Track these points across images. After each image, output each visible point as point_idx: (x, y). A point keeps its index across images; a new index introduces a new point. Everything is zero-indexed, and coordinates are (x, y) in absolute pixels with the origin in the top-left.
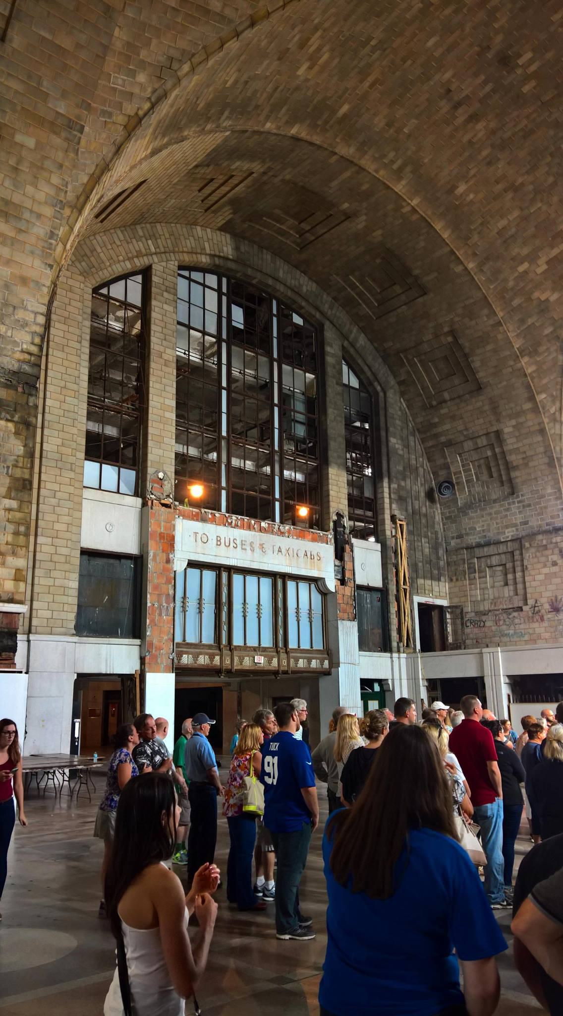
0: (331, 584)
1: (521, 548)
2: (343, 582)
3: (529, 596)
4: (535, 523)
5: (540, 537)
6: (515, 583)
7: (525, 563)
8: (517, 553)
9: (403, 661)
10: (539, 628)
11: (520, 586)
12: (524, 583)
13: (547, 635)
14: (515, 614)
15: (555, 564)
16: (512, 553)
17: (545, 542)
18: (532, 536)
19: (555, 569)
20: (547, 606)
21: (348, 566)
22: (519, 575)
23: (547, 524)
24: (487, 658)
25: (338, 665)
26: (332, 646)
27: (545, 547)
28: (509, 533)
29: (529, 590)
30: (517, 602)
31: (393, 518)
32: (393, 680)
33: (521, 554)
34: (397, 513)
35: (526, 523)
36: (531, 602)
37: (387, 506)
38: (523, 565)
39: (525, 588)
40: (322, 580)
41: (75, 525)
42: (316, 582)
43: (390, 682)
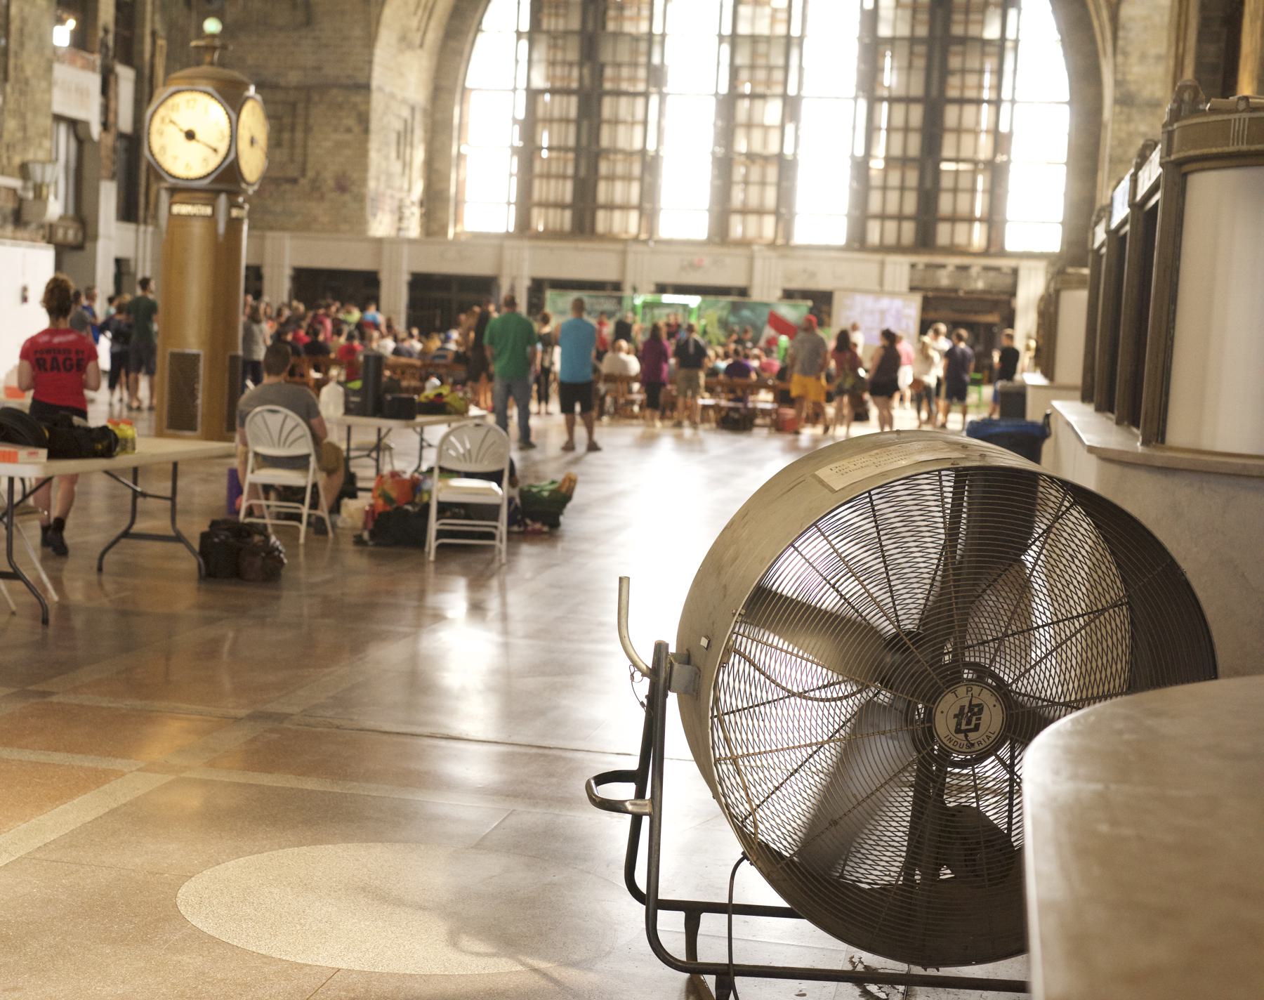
0: (96, 130)
1: (308, 100)
2: (105, 126)
3: (309, 165)
4: (331, 71)
5: (335, 91)
6: (292, 145)
7: (311, 121)
8: (300, 106)
9: (149, 237)
10: (317, 209)
11: (299, 151)
12: (305, 146)
13: (325, 219)
14: (287, 187)
15: (349, 130)
16: (294, 106)
17: (340, 99)
18: (324, 88)
19: (348, 137)
20: (331, 183)
21: (112, 105)
22: (299, 135)
23: (348, 77)
24: (269, 244)
25: (95, 238)
26: (86, 211)
27: (340, 106)
28: (294, 77)
29: (311, 159)
30: (292, 171)
31: (154, 34)
32: (136, 260)
33: (307, 108)
34: (158, 27)
35: (318, 68)
36: (311, 174)
37: (148, 16)
38: (306, 123)
39: (305, 155)
40: (86, 124)
41: (49, 104)
42: (74, 125)
43: (132, 263)
